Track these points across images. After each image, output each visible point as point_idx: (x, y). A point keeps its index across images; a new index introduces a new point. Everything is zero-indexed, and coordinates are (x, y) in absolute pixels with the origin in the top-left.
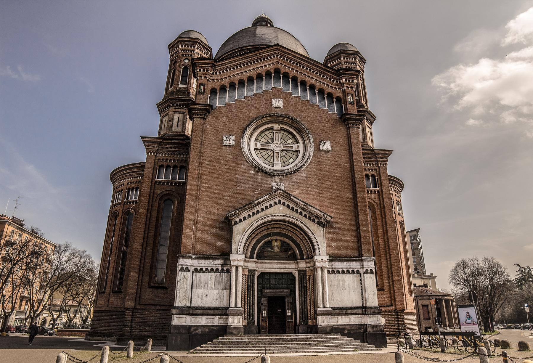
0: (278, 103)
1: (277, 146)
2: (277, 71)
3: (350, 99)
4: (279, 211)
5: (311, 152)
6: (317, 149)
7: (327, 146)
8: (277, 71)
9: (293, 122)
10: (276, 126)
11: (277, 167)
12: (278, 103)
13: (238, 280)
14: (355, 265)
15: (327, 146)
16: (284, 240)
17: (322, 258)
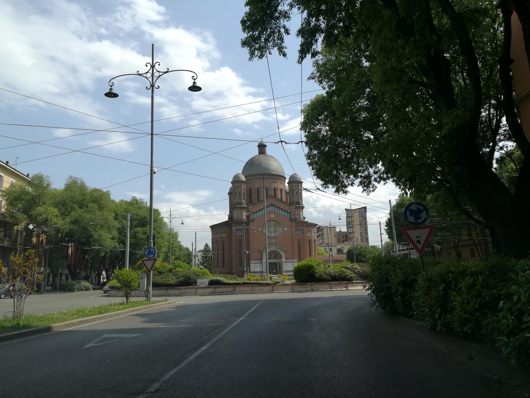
0: (272, 216)
1: (272, 229)
2: (272, 204)
3: (293, 213)
4: (273, 248)
5: (281, 231)
6: (283, 230)
7: (286, 229)
8: (272, 204)
9: (276, 222)
10: (272, 223)
11: (273, 235)
12: (272, 216)
13: (264, 265)
14: (292, 261)
15: (286, 229)
16: (275, 255)
17: (284, 260)
